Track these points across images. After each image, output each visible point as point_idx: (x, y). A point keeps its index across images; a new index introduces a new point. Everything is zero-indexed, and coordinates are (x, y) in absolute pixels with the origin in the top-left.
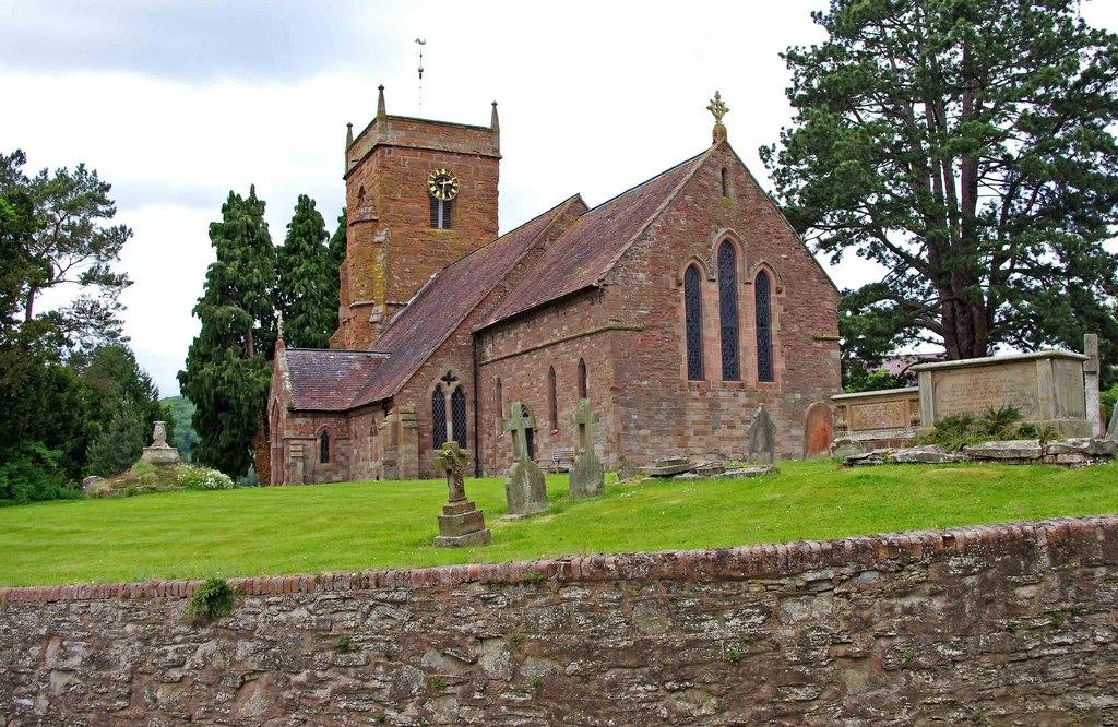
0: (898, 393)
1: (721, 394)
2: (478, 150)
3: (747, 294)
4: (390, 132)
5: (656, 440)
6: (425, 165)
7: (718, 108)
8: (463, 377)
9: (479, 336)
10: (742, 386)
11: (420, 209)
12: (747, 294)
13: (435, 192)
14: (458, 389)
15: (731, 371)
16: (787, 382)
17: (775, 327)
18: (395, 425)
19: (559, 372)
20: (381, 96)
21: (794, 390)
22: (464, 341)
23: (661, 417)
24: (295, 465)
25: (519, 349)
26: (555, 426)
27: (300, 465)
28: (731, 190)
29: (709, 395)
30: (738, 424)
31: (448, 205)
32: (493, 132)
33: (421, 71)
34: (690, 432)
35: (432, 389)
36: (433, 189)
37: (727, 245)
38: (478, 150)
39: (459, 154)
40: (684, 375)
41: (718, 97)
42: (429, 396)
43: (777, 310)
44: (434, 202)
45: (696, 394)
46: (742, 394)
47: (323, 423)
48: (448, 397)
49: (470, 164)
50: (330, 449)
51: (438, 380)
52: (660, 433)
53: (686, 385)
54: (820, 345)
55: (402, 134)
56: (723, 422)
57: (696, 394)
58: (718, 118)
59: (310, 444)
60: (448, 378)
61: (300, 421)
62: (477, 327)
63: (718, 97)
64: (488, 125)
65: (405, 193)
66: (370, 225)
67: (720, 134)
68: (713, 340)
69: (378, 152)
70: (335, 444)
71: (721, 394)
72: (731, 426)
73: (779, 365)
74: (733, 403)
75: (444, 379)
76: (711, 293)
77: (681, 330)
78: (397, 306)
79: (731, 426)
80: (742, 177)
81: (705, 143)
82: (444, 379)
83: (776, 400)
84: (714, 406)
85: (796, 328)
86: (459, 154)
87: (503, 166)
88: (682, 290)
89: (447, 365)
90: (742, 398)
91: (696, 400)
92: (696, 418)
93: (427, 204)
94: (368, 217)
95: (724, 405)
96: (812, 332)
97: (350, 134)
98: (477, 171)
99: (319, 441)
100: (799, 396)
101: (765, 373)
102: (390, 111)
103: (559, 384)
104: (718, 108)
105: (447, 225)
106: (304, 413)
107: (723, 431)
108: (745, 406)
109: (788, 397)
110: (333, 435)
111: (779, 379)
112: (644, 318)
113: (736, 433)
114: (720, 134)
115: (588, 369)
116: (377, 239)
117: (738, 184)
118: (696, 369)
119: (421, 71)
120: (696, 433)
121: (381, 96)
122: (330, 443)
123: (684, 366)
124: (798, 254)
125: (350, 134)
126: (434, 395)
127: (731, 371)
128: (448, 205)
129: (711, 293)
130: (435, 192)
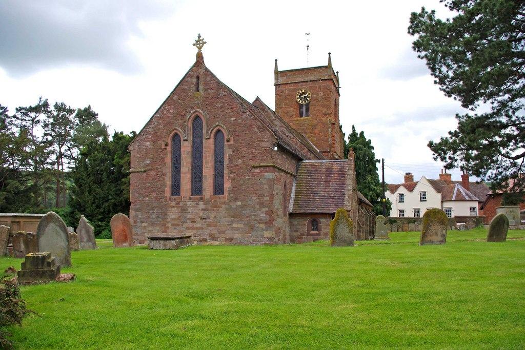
0: (30, 216)
1: (189, 203)
3: (209, 145)
4: (279, 79)
5: (151, 228)
7: (200, 43)
10: (201, 198)
12: (209, 145)
13: (299, 101)
15: (197, 189)
16: (232, 195)
20: (276, 64)
21: (236, 199)
23: (154, 216)
28: (201, 87)
29: (181, 204)
30: (198, 220)
31: (307, 105)
32: (329, 67)
33: (308, 47)
34: (169, 225)
36: (299, 99)
39: (311, 81)
41: (199, 37)
43: (228, 152)
44: (301, 106)
46: (201, 203)
49: (317, 85)
52: (153, 225)
53: (168, 199)
54: (257, 170)
55: (285, 78)
56: (189, 219)
57: (173, 204)
58: (200, 48)
63: (199, 37)
64: (326, 64)
65: (286, 104)
67: (200, 57)
68: (185, 173)
71: (189, 203)
72: (194, 221)
73: (227, 185)
74: (194, 208)
76: (186, 148)
77: (168, 169)
79: (194, 221)
80: (208, 79)
83: (223, 206)
84: (184, 210)
86: (311, 81)
90: (201, 205)
91: (174, 207)
92: (173, 217)
93: (297, 107)
95: (190, 210)
96: (252, 163)
98: (320, 87)
100: (239, 203)
101: (219, 189)
102: (280, 69)
104: (200, 43)
105: (307, 115)
107: (189, 224)
108: (203, 209)
109: (232, 204)
111: (226, 193)
112: (148, 165)
113: (196, 225)
114: (200, 57)
117: (206, 83)
118: (176, 189)
119: (308, 47)
120: (173, 225)
121: (276, 64)
123: (168, 189)
124: (244, 116)
127: (197, 189)
129: (186, 148)
130: (299, 101)
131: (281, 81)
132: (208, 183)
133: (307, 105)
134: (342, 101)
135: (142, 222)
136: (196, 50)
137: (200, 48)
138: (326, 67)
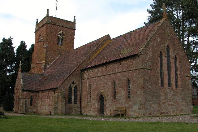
2: (69, 28)
3: (172, 61)
5: (153, 105)
6: (57, 29)
8: (77, 83)
9: (83, 71)
11: (56, 39)
12: (172, 61)
14: (76, 86)
15: (170, 85)
17: (178, 72)
18: (58, 96)
19: (117, 82)
22: (78, 72)
23: (155, 98)
24: (23, 106)
25: (99, 75)
26: (115, 98)
27: (24, 106)
33: (57, 8)
34: (161, 103)
35: (69, 86)
37: (168, 46)
38: (69, 28)
39: (66, 27)
40: (160, 85)
44: (58, 38)
45: (162, 91)
47: (31, 94)
48: (73, 89)
50: (33, 102)
51: (70, 83)
56: (168, 100)
57: (162, 91)
59: (27, 100)
60: (73, 83)
61: (25, 93)
62: (82, 68)
64: (73, 21)
66: (42, 43)
68: (166, 75)
69: (46, 25)
70: (34, 100)
72: (170, 101)
74: (170, 93)
75: (72, 83)
76: (165, 59)
78: (48, 64)
82: (72, 83)
86: (66, 27)
87: (76, 32)
89: (73, 79)
92: (163, 98)
93: (57, 39)
94: (42, 41)
97: (37, 21)
98: (70, 32)
99: (30, 99)
103: (117, 86)
105: (61, 45)
106: (26, 91)
108: (173, 95)
110: (34, 98)
111: (180, 88)
115: (131, 82)
116: (44, 46)
119: (57, 8)
120: (163, 103)
122: (33, 100)
125: (37, 21)
126: (69, 88)
127: (170, 85)
128: (62, 40)
129: (165, 59)
131: (50, 21)
133: (62, 40)
135: (149, 101)
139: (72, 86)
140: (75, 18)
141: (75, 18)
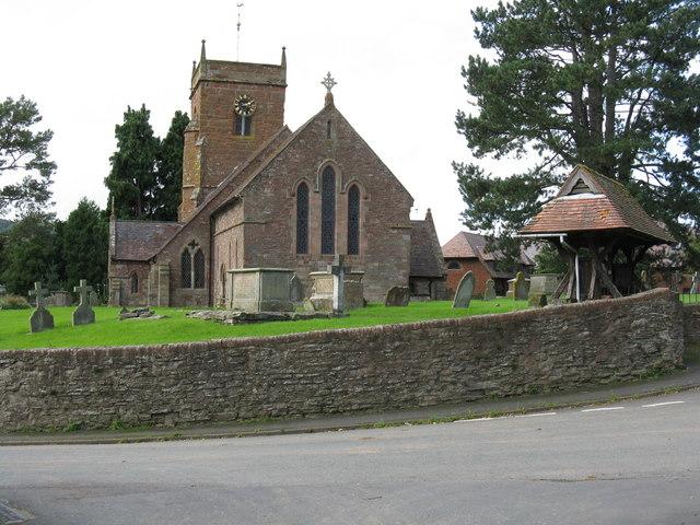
2: (270, 80)
3: (341, 201)
6: (232, 93)
7: (329, 82)
8: (202, 243)
9: (214, 218)
11: (229, 122)
12: (341, 201)
15: (327, 247)
17: (361, 221)
22: (204, 221)
24: (114, 294)
27: (118, 294)
32: (282, 68)
33: (239, 25)
35: (182, 251)
36: (237, 109)
38: (270, 80)
41: (329, 75)
42: (180, 255)
43: (363, 208)
44: (238, 118)
45: (301, 262)
47: (134, 268)
48: (192, 256)
49: (265, 91)
54: (395, 231)
57: (301, 262)
58: (329, 88)
59: (125, 281)
60: (193, 244)
61: (118, 266)
63: (329, 75)
64: (279, 63)
66: (193, 134)
67: (329, 98)
73: (363, 245)
76: (315, 201)
77: (293, 223)
78: (210, 188)
81: (320, 105)
85: (378, 221)
87: (288, 92)
88: (295, 199)
91: (300, 266)
98: (269, 95)
102: (208, 57)
104: (329, 82)
105: (247, 132)
106: (122, 261)
112: (268, 216)
114: (329, 98)
116: (198, 144)
118: (302, 246)
119: (239, 25)
123: (294, 245)
126: (184, 254)
127: (327, 247)
128: (248, 119)
129: (315, 201)
131: (210, 75)
132: (315, 240)
133: (248, 119)
134: (285, 114)
136: (325, 91)
137: (329, 88)
138: (279, 67)
139: (190, 251)
140: (284, 53)
141: (284, 53)
